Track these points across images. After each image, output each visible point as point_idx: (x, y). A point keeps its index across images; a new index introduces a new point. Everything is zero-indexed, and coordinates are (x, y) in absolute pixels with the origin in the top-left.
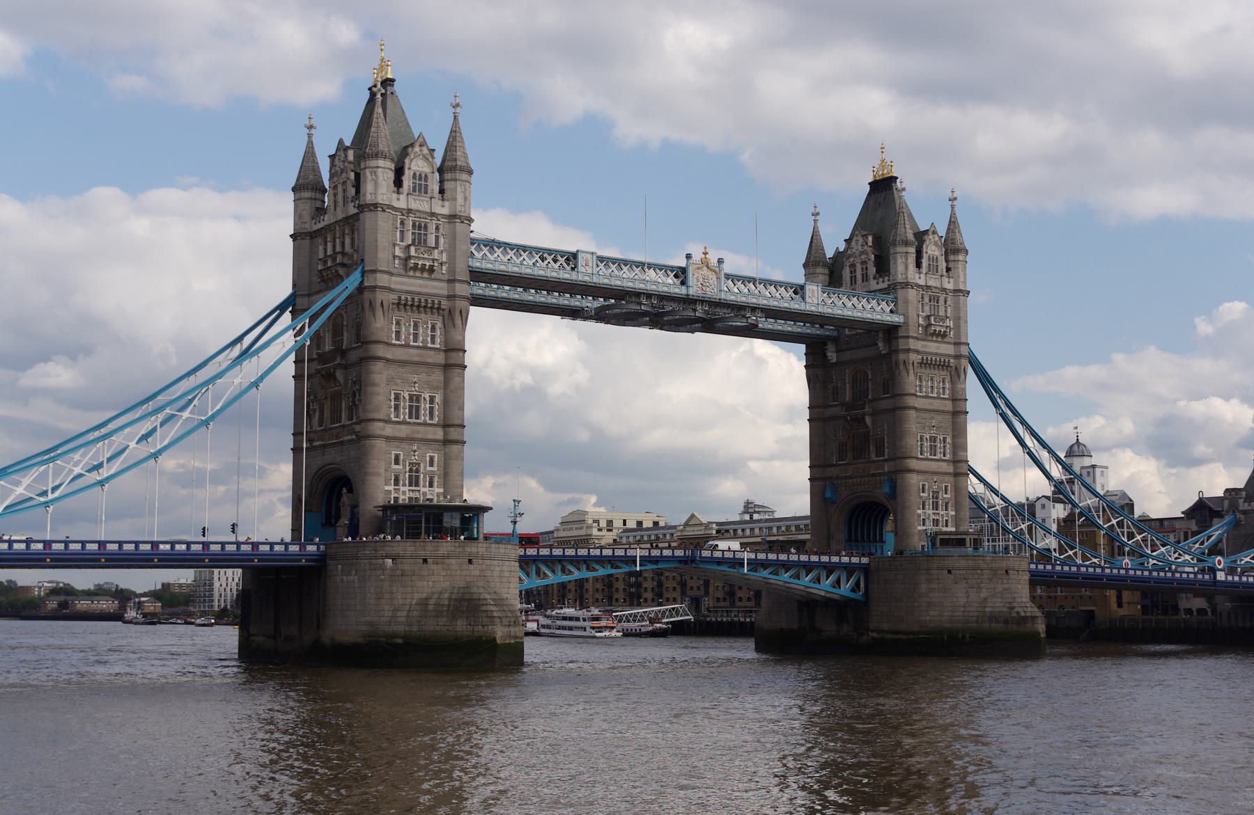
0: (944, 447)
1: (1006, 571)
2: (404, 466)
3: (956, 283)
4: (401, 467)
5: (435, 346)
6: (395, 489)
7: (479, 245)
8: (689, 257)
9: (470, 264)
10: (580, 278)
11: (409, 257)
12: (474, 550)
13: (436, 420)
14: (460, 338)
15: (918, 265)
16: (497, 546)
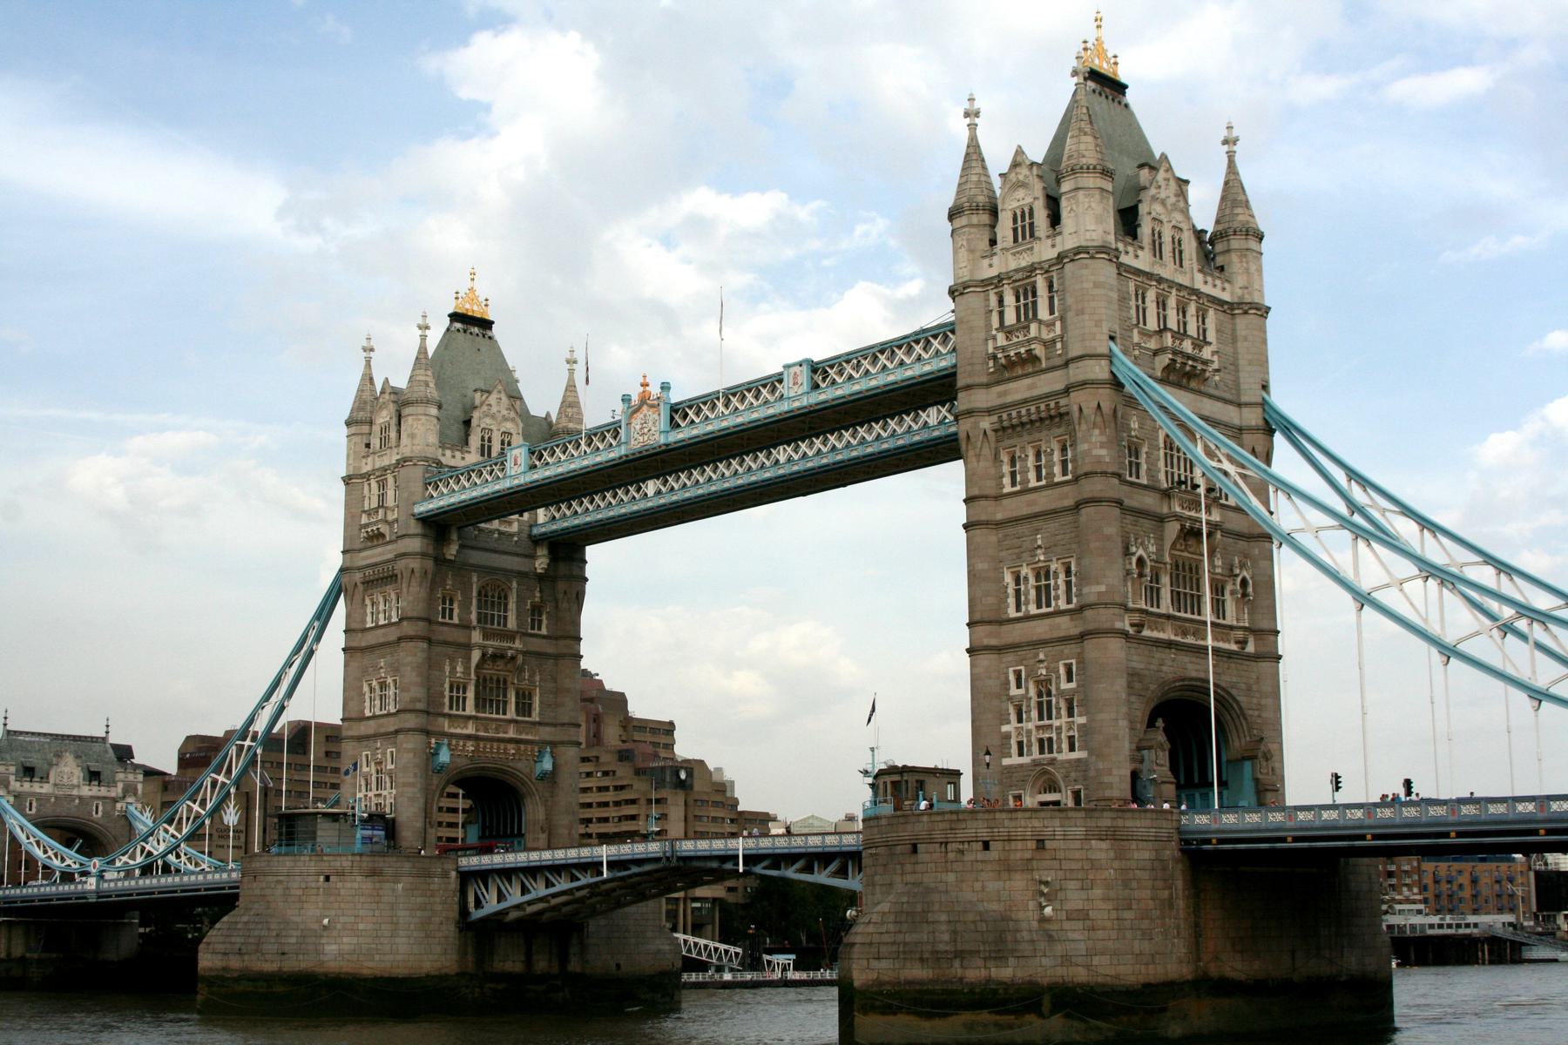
0: (1068, 584)
4: (368, 769)
8: (626, 399)
12: (258, 864)
15: (993, 242)
16: (281, 858)
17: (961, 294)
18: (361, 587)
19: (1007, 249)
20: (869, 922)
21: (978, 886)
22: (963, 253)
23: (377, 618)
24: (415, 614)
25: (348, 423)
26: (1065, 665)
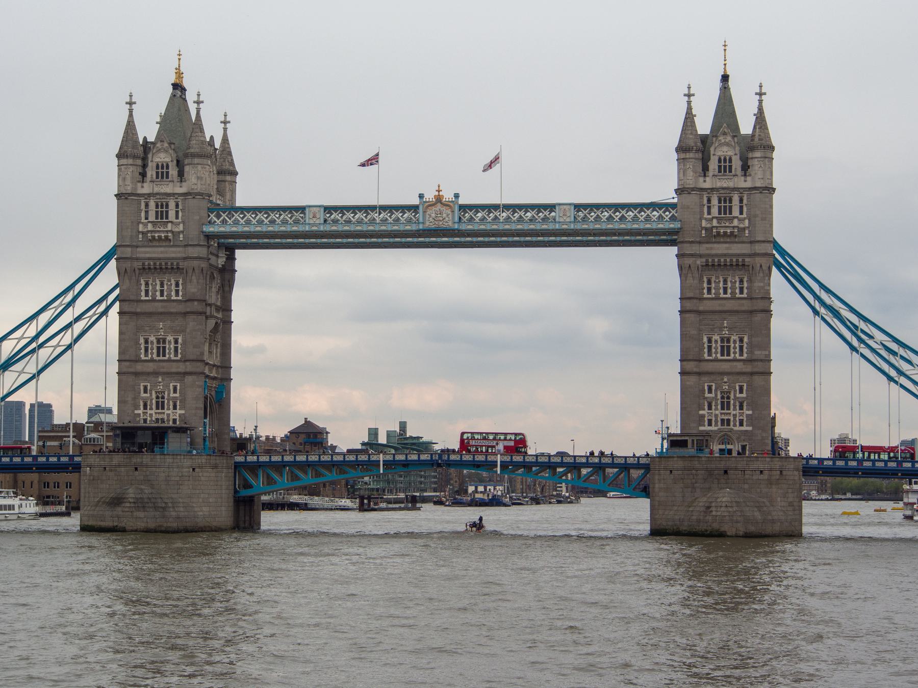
0: (741, 348)
1: (726, 472)
2: (151, 394)
3: (753, 180)
4: (148, 395)
5: (178, 298)
6: (143, 413)
7: (218, 212)
8: (421, 196)
9: (204, 229)
10: (307, 228)
11: (148, 231)
12: (138, 460)
13: (180, 356)
14: (195, 290)
15: (705, 169)
16: (162, 457)
17: (690, 193)
18: (137, 272)
19: (716, 176)
20: (726, 506)
21: (759, 490)
22: (690, 173)
23: (154, 295)
24: (202, 298)
25: (119, 156)
26: (739, 385)
